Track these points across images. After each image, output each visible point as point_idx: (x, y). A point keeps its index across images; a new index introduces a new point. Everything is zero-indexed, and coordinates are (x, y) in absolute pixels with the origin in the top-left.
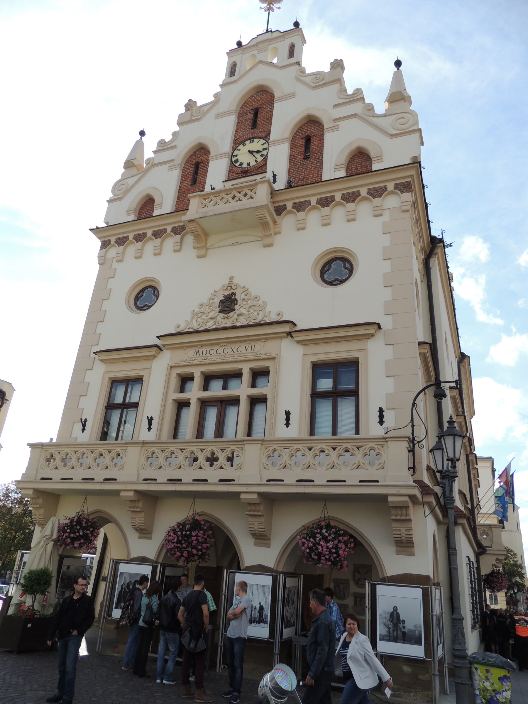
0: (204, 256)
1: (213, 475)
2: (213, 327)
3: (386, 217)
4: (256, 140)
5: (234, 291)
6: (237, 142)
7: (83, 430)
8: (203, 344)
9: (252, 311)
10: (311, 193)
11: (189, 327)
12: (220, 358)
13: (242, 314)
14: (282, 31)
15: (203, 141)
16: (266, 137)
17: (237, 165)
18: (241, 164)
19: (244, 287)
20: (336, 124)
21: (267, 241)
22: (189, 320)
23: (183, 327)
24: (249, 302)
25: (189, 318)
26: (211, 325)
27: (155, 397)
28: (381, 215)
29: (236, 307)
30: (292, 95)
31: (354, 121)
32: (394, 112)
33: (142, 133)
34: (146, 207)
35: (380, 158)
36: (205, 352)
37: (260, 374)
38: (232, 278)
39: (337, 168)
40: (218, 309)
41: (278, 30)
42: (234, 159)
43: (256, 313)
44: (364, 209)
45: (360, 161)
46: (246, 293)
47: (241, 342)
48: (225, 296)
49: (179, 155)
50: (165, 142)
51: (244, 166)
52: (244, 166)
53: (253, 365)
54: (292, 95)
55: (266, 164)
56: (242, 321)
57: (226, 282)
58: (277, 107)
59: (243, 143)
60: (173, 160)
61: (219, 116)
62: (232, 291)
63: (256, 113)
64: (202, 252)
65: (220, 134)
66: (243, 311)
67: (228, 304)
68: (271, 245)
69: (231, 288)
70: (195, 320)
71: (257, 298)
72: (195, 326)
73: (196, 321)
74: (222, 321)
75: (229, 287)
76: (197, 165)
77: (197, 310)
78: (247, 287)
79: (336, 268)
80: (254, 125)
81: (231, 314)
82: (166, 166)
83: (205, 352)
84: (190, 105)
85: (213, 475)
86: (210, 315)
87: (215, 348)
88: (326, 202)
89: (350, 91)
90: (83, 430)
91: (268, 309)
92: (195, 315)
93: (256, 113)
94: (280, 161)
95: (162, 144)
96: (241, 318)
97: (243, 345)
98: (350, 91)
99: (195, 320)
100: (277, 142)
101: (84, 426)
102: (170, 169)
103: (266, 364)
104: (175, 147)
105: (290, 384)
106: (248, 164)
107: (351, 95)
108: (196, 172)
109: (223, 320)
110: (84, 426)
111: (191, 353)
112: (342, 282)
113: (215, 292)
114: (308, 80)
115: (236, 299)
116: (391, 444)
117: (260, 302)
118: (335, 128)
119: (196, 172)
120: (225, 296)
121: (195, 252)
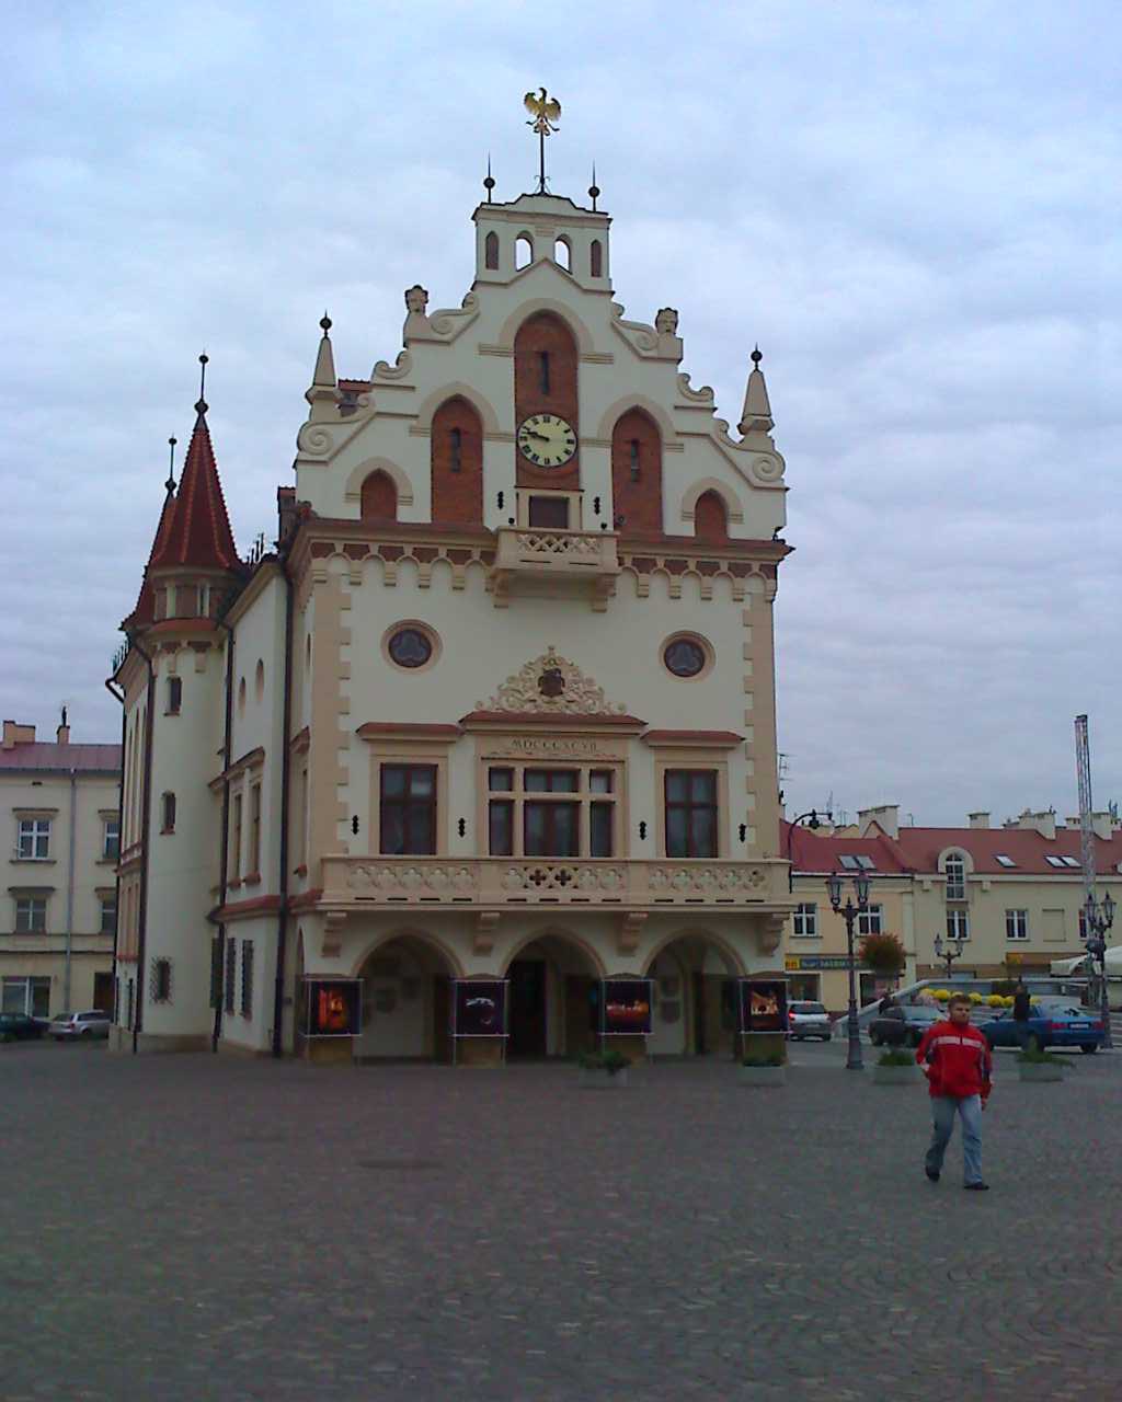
0: (506, 607)
2: (534, 712)
3: (746, 605)
4: (554, 419)
5: (559, 667)
7: (355, 831)
8: (528, 734)
9: (585, 698)
11: (496, 706)
12: (546, 751)
14: (577, 206)
15: (465, 394)
16: (571, 418)
17: (529, 456)
18: (536, 457)
19: (572, 665)
20: (679, 440)
21: (598, 606)
22: (496, 698)
23: (487, 706)
24: (581, 685)
25: (495, 693)
26: (528, 707)
27: (462, 793)
28: (742, 600)
29: (564, 689)
30: (607, 359)
31: (704, 442)
32: (755, 448)
33: (326, 323)
34: (379, 488)
35: (739, 518)
36: (528, 744)
38: (551, 649)
39: (685, 516)
40: (540, 689)
41: (569, 199)
42: (522, 444)
43: (590, 701)
44: (721, 588)
45: (711, 506)
46: (575, 673)
47: (577, 737)
48: (546, 672)
50: (389, 370)
51: (541, 462)
52: (541, 462)
53: (594, 766)
54: (607, 359)
55: (577, 471)
56: (574, 709)
57: (546, 652)
59: (532, 415)
60: (416, 417)
62: (555, 666)
64: (500, 601)
65: (495, 389)
66: (575, 697)
67: (551, 682)
68: (604, 611)
69: (555, 663)
70: (504, 699)
71: (590, 682)
72: (509, 704)
73: (508, 701)
74: (544, 705)
77: (506, 685)
78: (575, 664)
79: (686, 655)
80: (547, 387)
81: (557, 698)
83: (528, 744)
84: (416, 298)
86: (527, 696)
87: (543, 741)
88: (676, 567)
89: (695, 386)
90: (355, 831)
91: (607, 698)
92: (503, 692)
94: (597, 471)
96: (572, 705)
97: (581, 741)
98: (695, 386)
99: (504, 699)
101: (355, 824)
102: (413, 431)
103: (611, 766)
104: (413, 388)
105: (642, 796)
106: (547, 461)
107: (691, 392)
109: (545, 705)
110: (355, 824)
111: (508, 742)
112: (694, 674)
113: (531, 664)
114: (632, 336)
115: (563, 680)
116: (775, 869)
117: (596, 688)
118: (681, 447)
120: (546, 672)
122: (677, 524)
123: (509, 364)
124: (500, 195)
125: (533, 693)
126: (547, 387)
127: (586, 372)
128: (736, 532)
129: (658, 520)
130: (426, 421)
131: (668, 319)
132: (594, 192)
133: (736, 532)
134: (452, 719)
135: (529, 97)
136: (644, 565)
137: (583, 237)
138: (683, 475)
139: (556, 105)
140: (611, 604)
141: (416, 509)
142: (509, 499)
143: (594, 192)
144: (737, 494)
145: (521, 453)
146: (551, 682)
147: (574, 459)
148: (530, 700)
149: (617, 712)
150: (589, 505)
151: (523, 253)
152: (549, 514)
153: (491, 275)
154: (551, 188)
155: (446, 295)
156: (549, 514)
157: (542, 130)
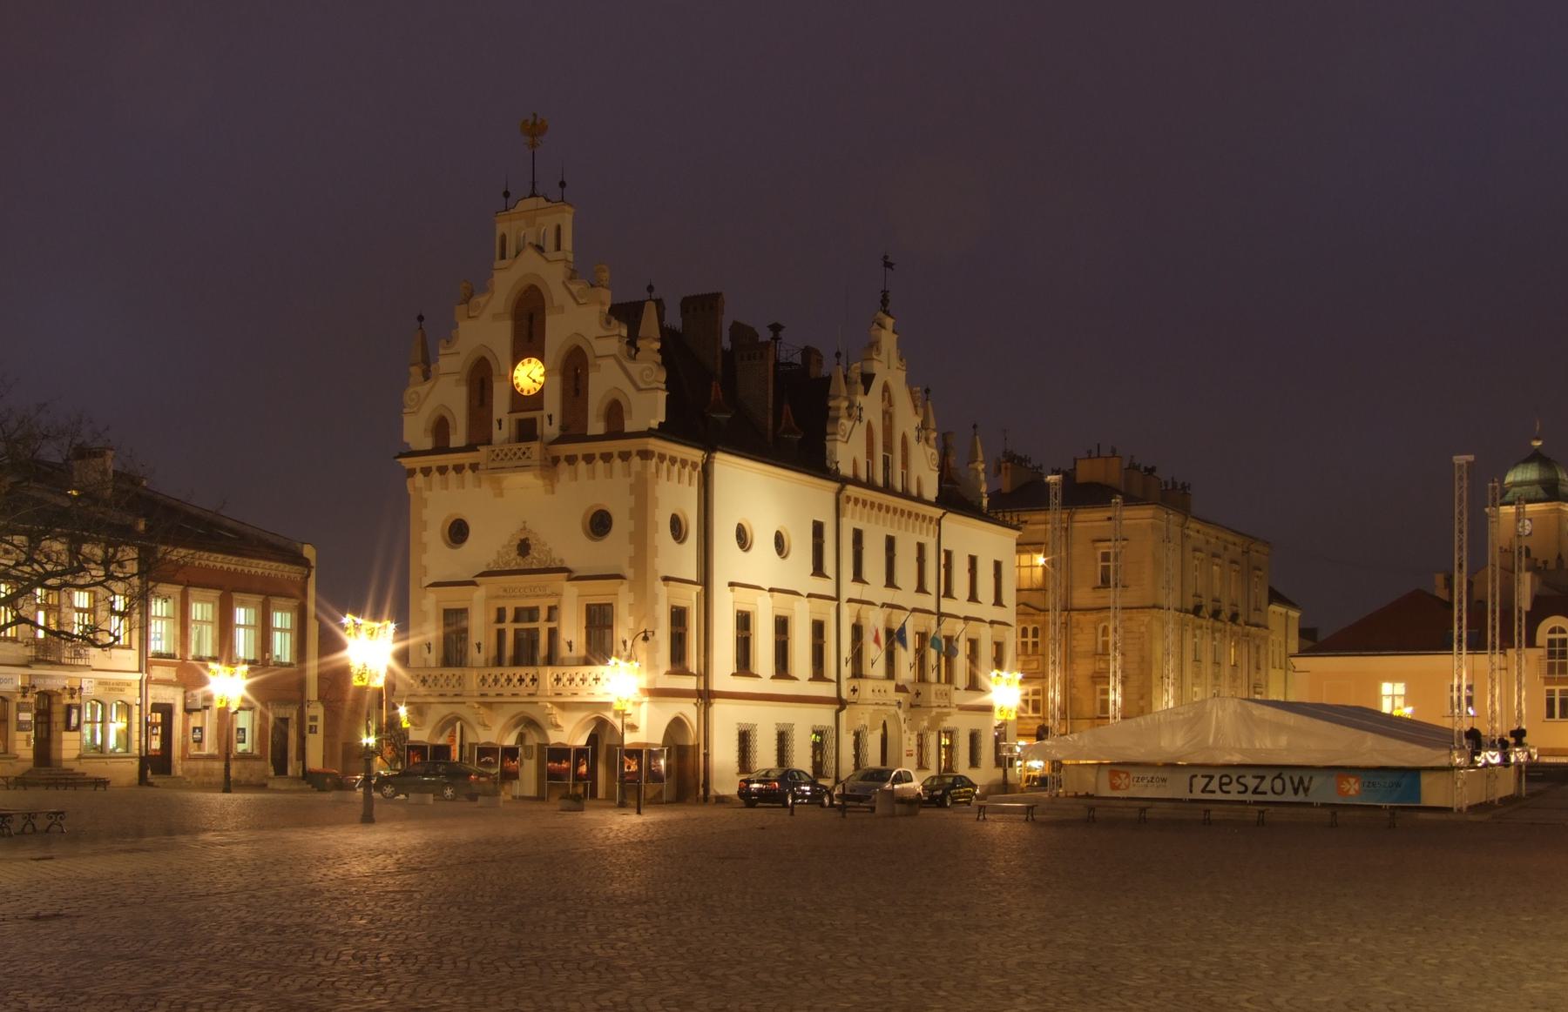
10: (578, 449)
13: (534, 559)
34: (441, 428)
37: (552, 612)
67: (524, 548)
71: (545, 544)
76: (482, 381)
80: (530, 336)
108: (482, 387)
119: (482, 387)
122: (596, 426)
125: (514, 554)
128: (629, 426)
129: (586, 427)
133: (629, 426)
134: (469, 578)
141: (458, 438)
142: (505, 424)
146: (524, 548)
148: (515, 561)
149: (559, 564)
150: (546, 420)
157: (533, 145)
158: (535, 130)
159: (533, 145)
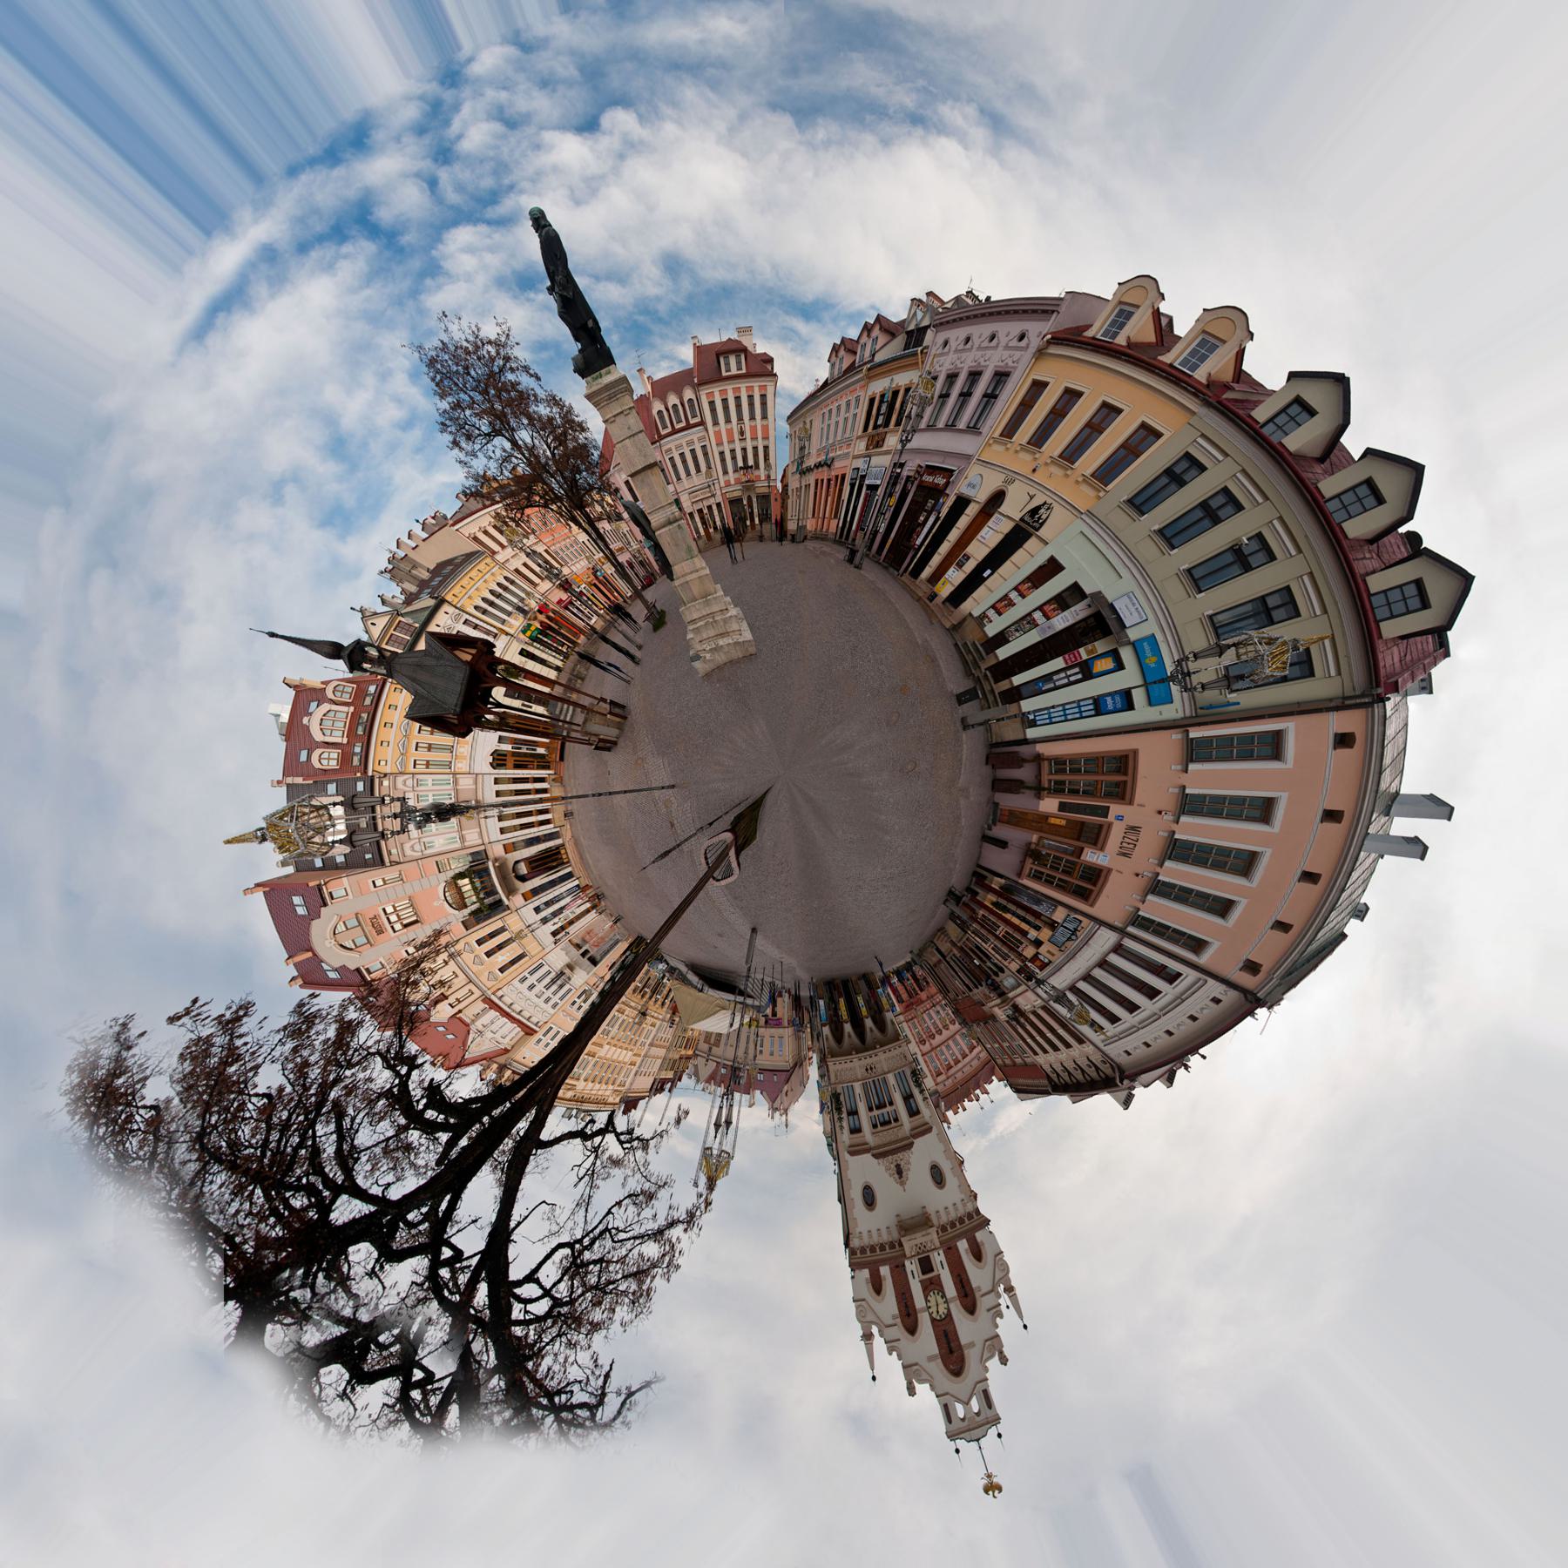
1: (869, 1061)
6: (949, 1315)
16: (933, 1320)
30: (931, 1359)
49: (983, 1303)
58: (936, 1351)
61: (972, 1345)
63: (951, 1352)
75: (903, 1184)
82: (984, 1290)
85: (869, 1061)
93: (951, 1352)
95: (1001, 1316)
100: (922, 1310)
114: (925, 1376)
118: (894, 1317)
121: (931, 1210)
123: (963, 1341)
124: (993, 1432)
126: (946, 1334)
127: (934, 1349)
130: (977, 1295)
131: (911, 1391)
132: (957, 1451)
135: (1000, 1490)
136: (892, 1245)
137: (956, 1425)
138: (888, 1305)
139: (986, 1491)
140: (892, 1222)
143: (957, 1451)
144: (867, 1292)
145: (944, 1296)
147: (927, 1301)
151: (975, 1405)
152: (926, 1265)
153: (980, 1387)
154: (974, 1444)
155: (994, 1363)
156: (926, 1265)
157: (989, 1476)
158: (992, 1487)
159: (989, 1476)
